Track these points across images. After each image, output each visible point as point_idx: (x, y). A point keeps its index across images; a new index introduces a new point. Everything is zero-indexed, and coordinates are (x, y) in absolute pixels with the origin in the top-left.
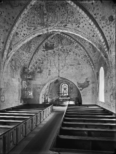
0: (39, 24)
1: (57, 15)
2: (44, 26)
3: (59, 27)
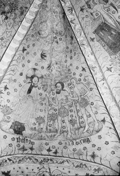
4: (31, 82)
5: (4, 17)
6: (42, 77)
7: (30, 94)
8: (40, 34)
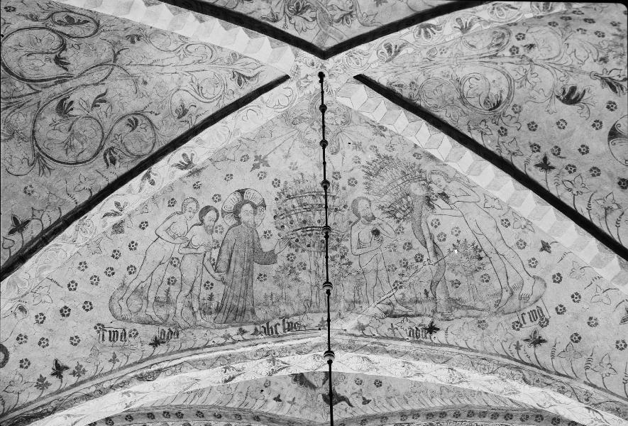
0: (205, 311)
1: (355, 265)
2: (244, 328)
5: (440, 202)
8: (499, 103)
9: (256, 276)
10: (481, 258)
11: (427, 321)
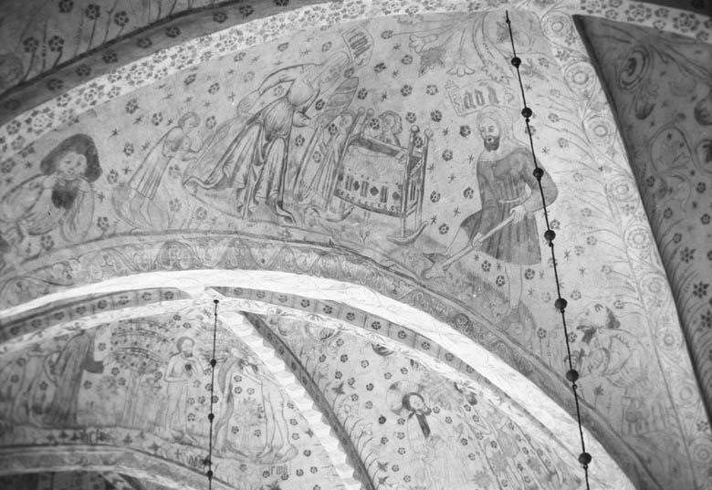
0: (37, 410)
1: (163, 391)
3: (162, 457)
4: (411, 412)
5: (250, 369)
6: (422, 387)
7: (432, 433)
9: (83, 382)
10: (260, 417)
11: (205, 454)
